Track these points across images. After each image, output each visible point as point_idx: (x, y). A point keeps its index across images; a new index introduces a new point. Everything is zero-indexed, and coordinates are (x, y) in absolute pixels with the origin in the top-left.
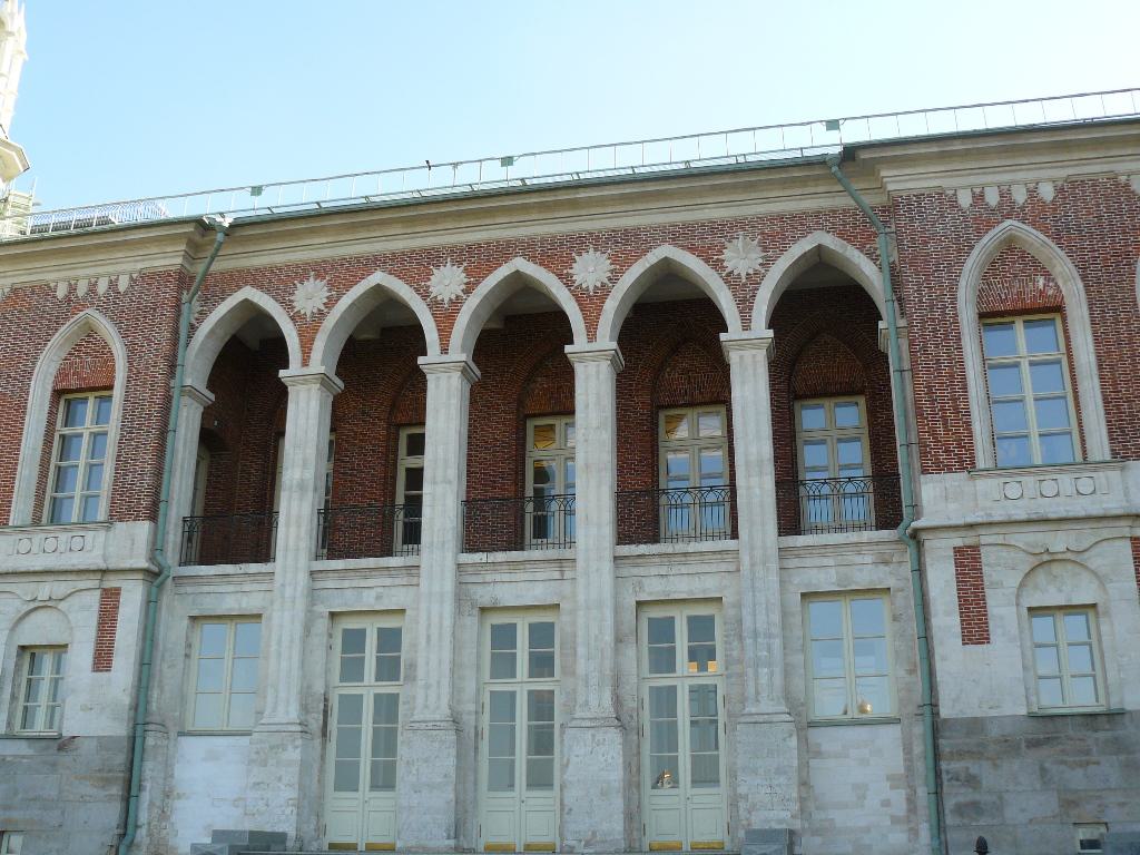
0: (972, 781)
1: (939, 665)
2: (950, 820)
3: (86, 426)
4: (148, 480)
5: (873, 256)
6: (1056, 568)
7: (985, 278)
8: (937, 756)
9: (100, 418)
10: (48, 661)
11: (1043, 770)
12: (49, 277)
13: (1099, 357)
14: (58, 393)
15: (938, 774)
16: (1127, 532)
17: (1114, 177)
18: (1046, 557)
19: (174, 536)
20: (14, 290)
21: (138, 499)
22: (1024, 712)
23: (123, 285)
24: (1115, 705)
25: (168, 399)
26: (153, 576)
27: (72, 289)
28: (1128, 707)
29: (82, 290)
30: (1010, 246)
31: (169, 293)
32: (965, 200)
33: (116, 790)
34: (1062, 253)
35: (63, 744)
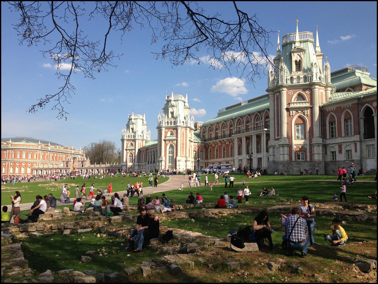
3: (349, 123)
4: (358, 130)
9: (351, 122)
10: (350, 151)
12: (341, 105)
14: (345, 120)
19: (362, 136)
20: (337, 107)
21: (357, 132)
23: (350, 106)
25: (359, 119)
26: (360, 141)
27: (344, 107)
29: (345, 107)
31: (356, 106)
33: (360, 165)
35: (353, 161)
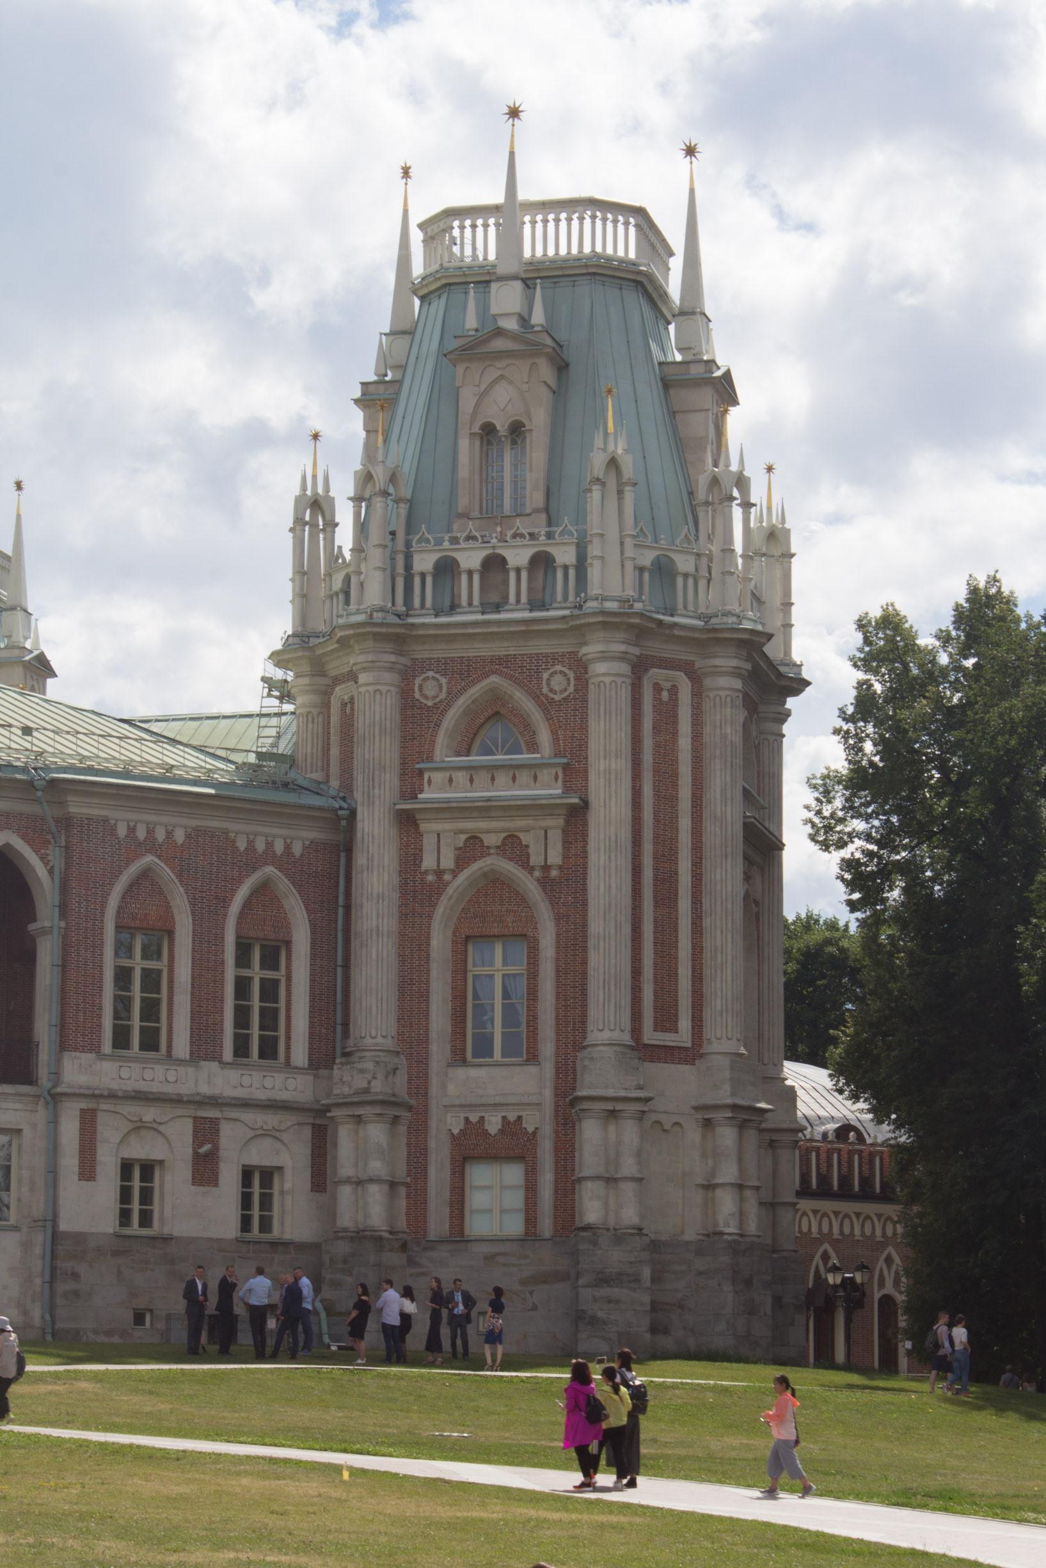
0: (75, 1276)
1: (62, 1193)
2: (60, 1301)
5: (43, 858)
6: (143, 1132)
7: (123, 897)
8: (54, 1255)
11: (119, 1271)
13: (193, 978)
15: (53, 1269)
16: (192, 1112)
17: (226, 832)
18: (138, 1124)
22: (111, 1231)
24: (166, 1231)
28: (176, 1234)
30: (146, 874)
32: (122, 831)
34: (181, 889)
